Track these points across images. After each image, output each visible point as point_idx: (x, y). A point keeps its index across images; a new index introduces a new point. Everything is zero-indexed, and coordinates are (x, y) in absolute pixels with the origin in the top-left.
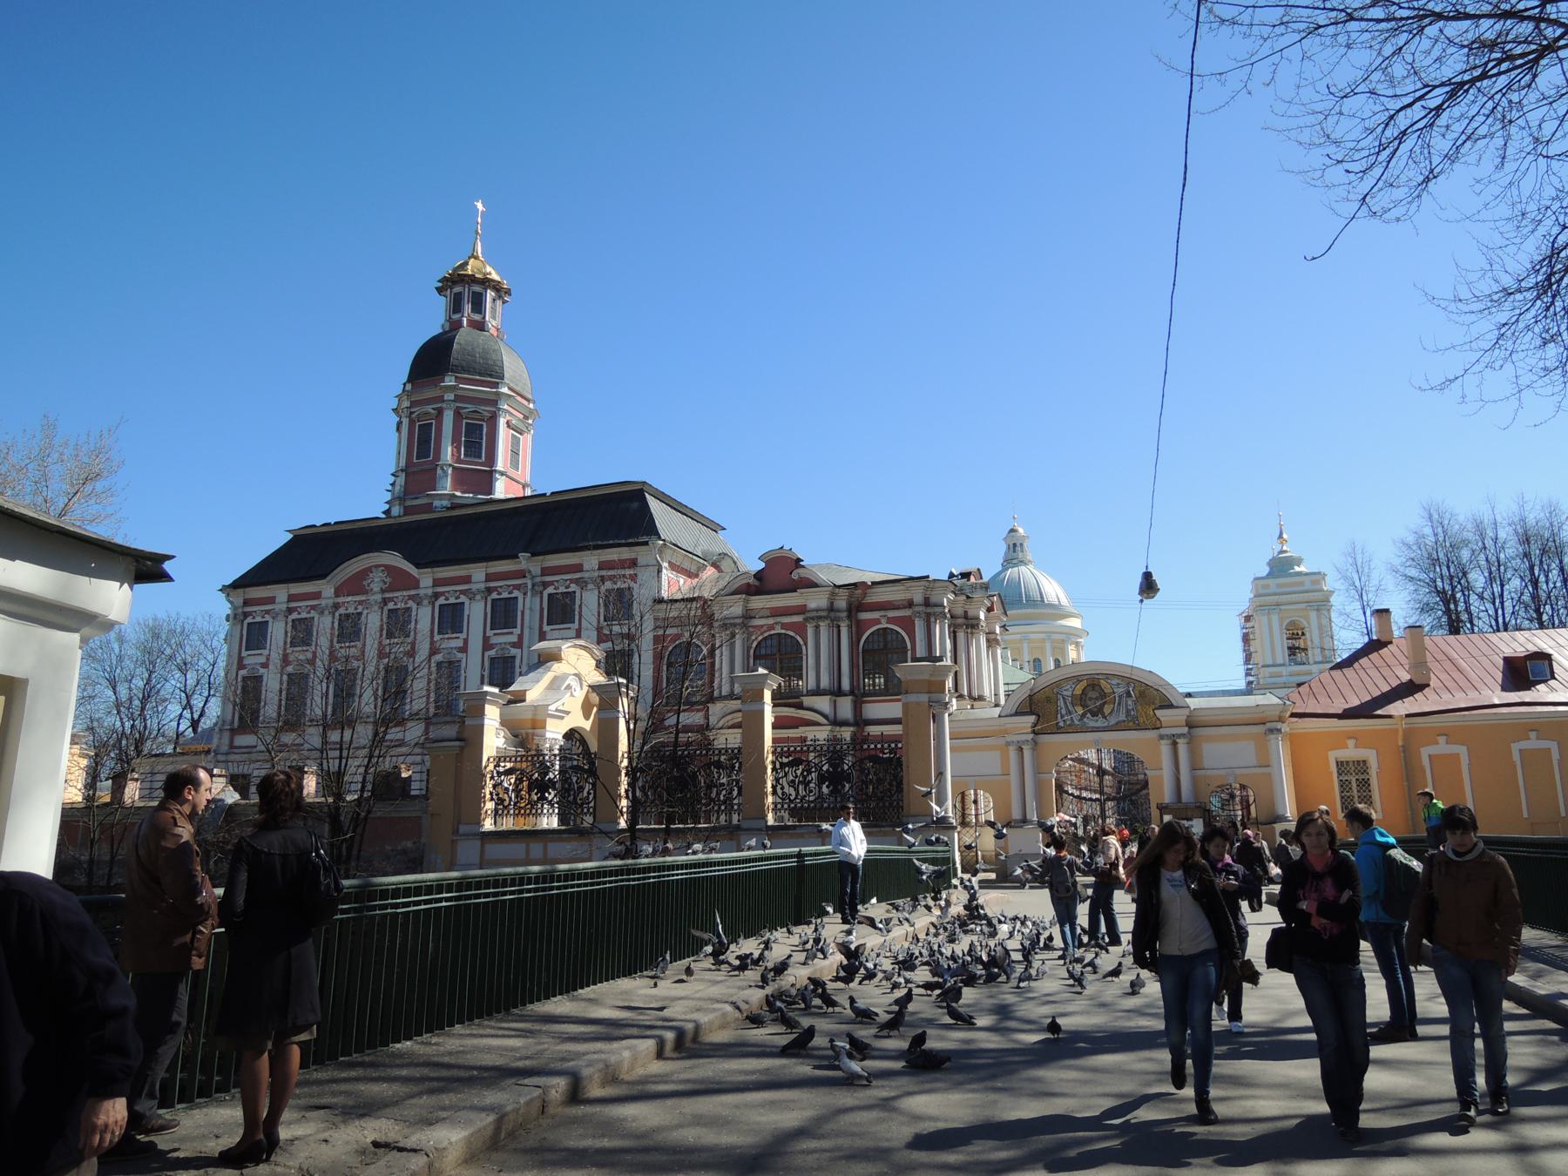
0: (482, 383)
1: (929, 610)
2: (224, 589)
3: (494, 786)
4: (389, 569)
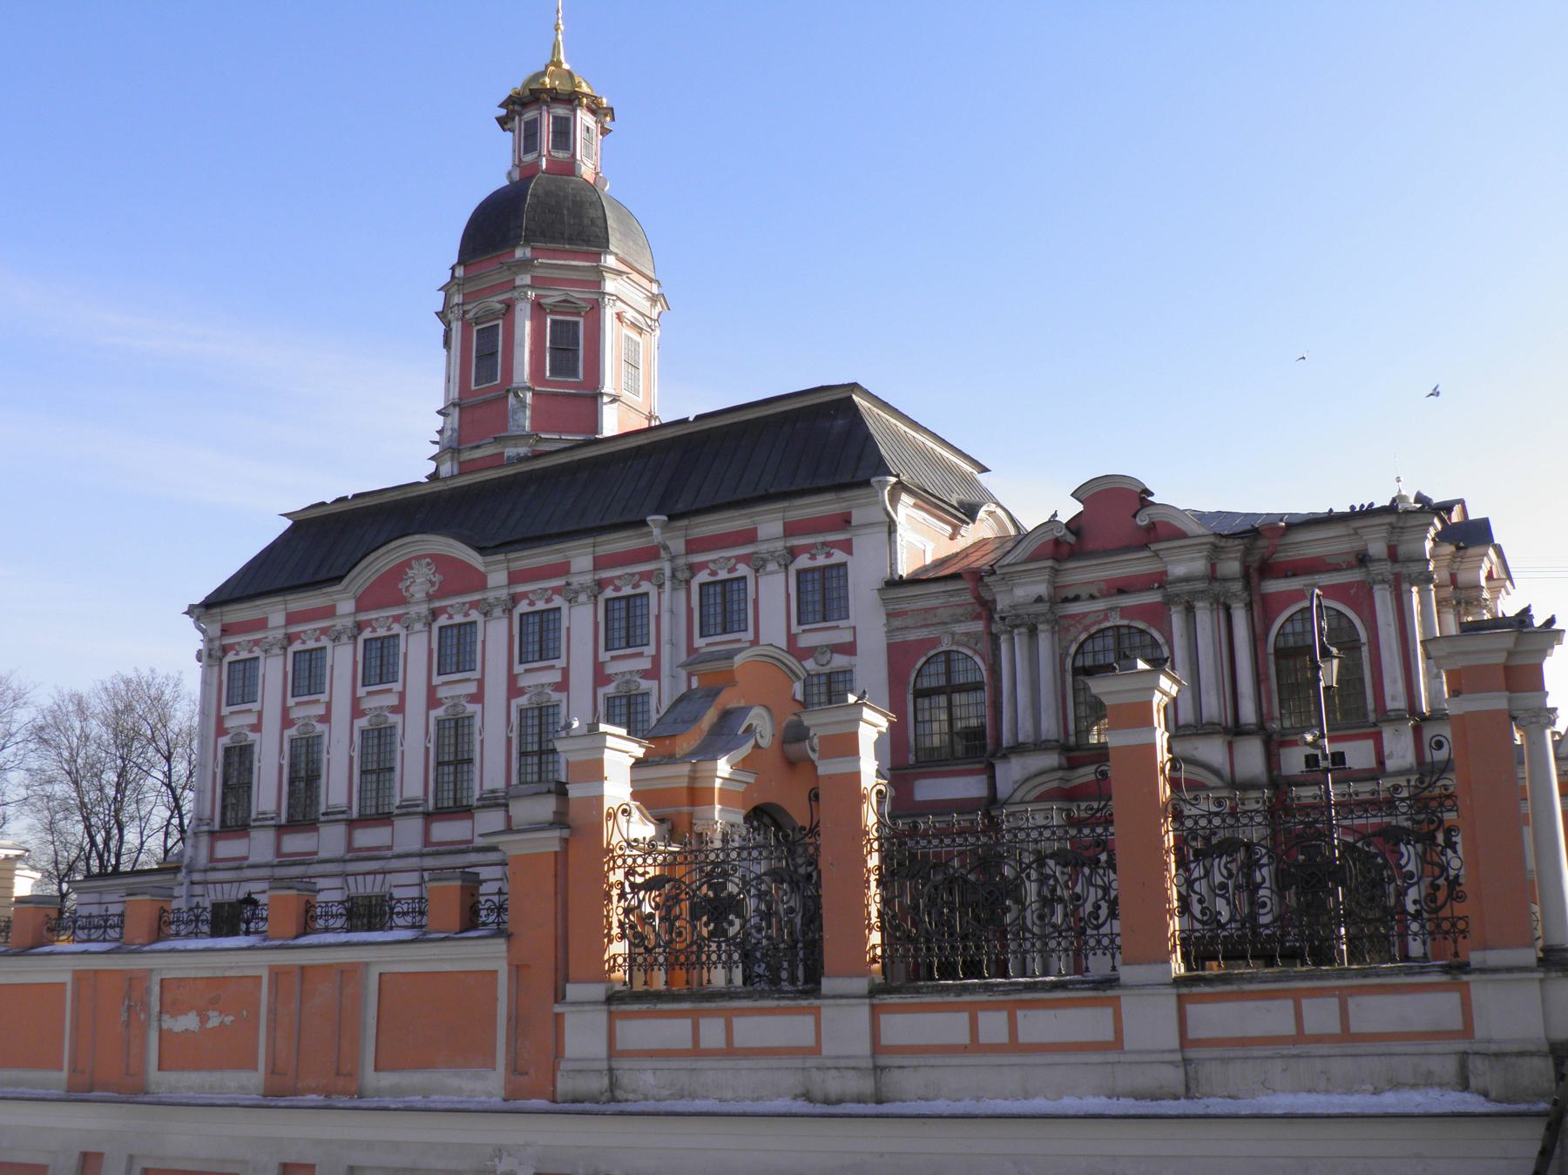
0: (575, 255)
1: (1398, 568)
2: (191, 611)
3: (627, 911)
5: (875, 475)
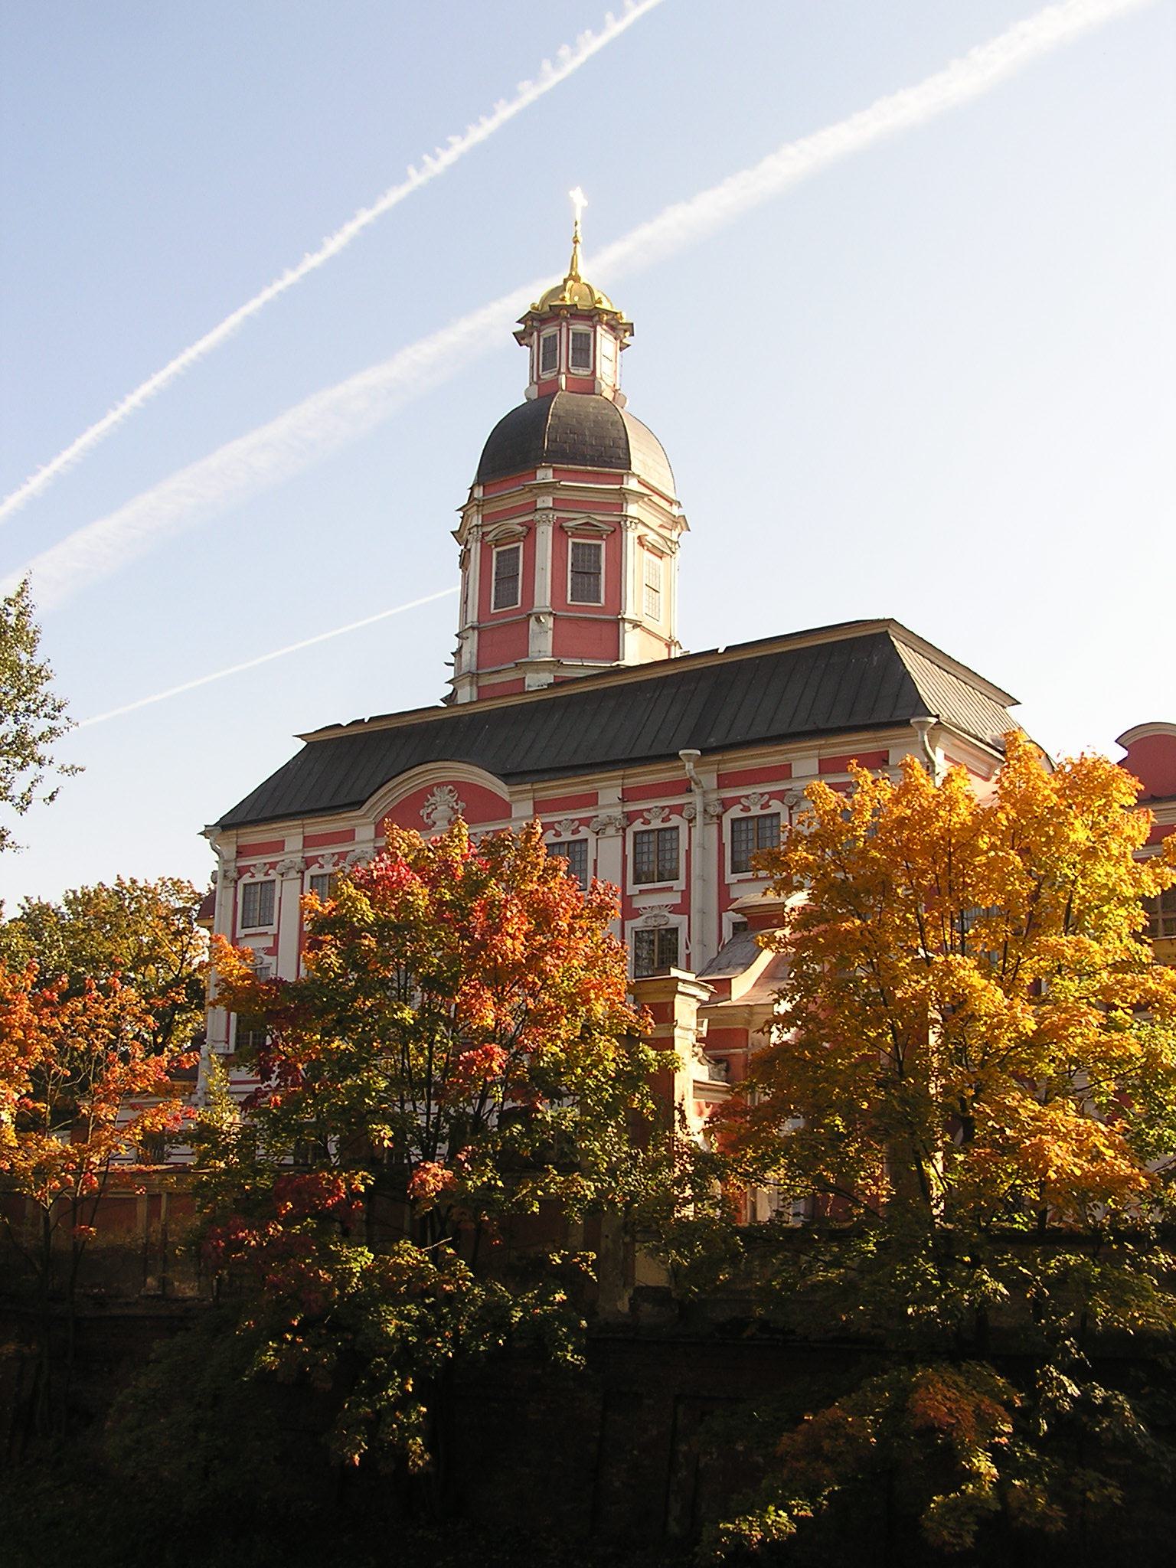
4: (462, 789)
5: (913, 715)
